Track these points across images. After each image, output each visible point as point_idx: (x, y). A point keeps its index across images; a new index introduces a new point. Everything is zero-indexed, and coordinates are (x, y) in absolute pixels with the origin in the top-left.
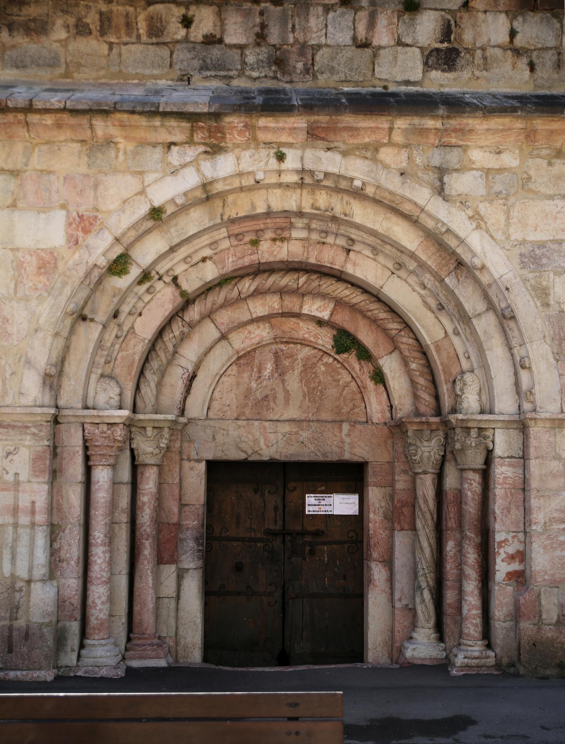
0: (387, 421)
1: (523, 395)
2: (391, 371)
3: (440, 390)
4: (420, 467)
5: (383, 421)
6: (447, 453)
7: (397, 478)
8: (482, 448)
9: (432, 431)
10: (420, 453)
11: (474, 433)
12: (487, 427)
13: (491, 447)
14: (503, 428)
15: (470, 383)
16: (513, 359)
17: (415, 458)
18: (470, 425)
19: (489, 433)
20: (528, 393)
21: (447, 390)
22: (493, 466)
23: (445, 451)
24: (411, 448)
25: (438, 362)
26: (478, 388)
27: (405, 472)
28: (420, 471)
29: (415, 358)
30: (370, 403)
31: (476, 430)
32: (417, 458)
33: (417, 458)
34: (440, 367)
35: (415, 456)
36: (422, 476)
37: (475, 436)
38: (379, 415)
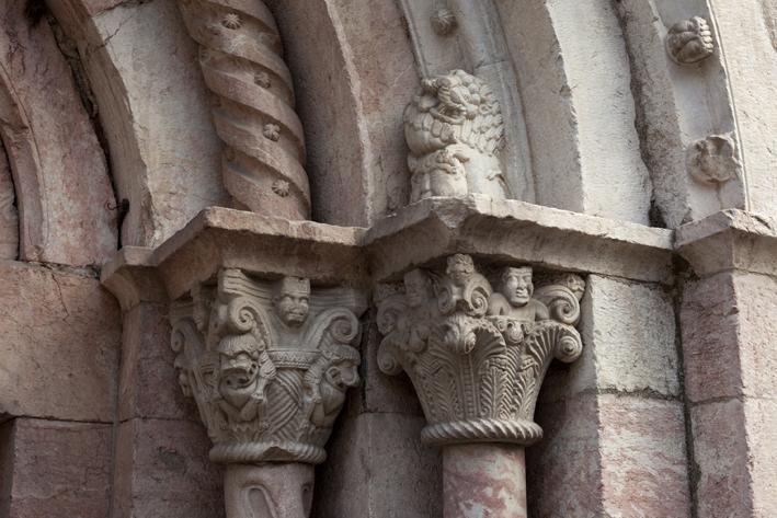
0: (102, 260)
1: (679, 162)
2: (136, 67)
3: (332, 144)
4: (254, 437)
5: (83, 258)
6: (371, 380)
7: (138, 483)
8: (541, 352)
9: (316, 287)
10: (267, 368)
11: (519, 280)
12: (565, 264)
13: (574, 343)
14: (617, 278)
15: (473, 108)
16: (625, 37)
17: (242, 392)
18: (509, 250)
19: (567, 292)
20: (710, 147)
21: (372, 136)
22: (576, 428)
23: (361, 371)
24: (239, 344)
25: (339, 28)
26: (497, 132)
27: (168, 459)
28: (258, 449)
29: (244, 18)
30: (36, 184)
31: (527, 272)
32: (256, 391)
33: (256, 391)
34: (346, 50)
35: (244, 383)
36: (265, 475)
37: (523, 296)
38: (72, 237)
